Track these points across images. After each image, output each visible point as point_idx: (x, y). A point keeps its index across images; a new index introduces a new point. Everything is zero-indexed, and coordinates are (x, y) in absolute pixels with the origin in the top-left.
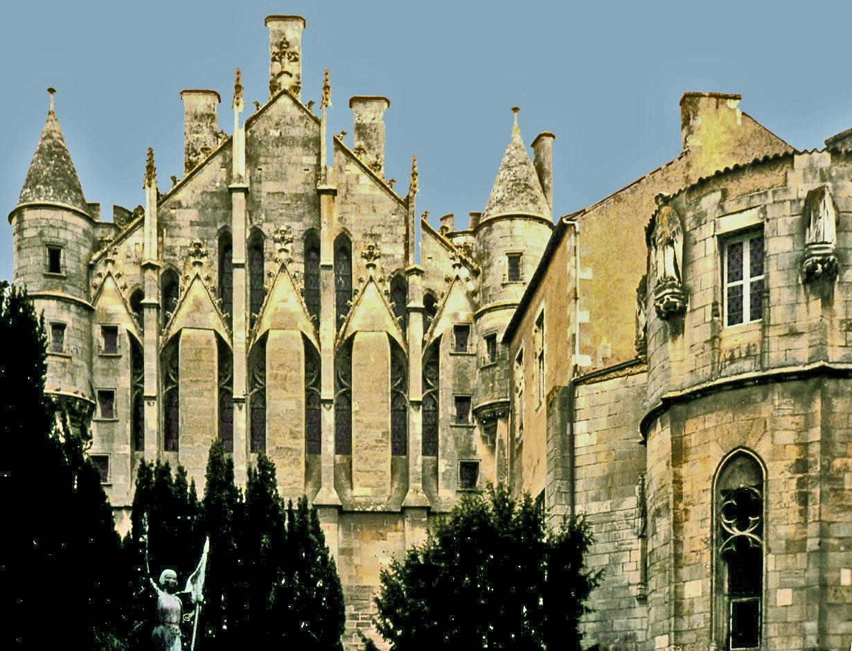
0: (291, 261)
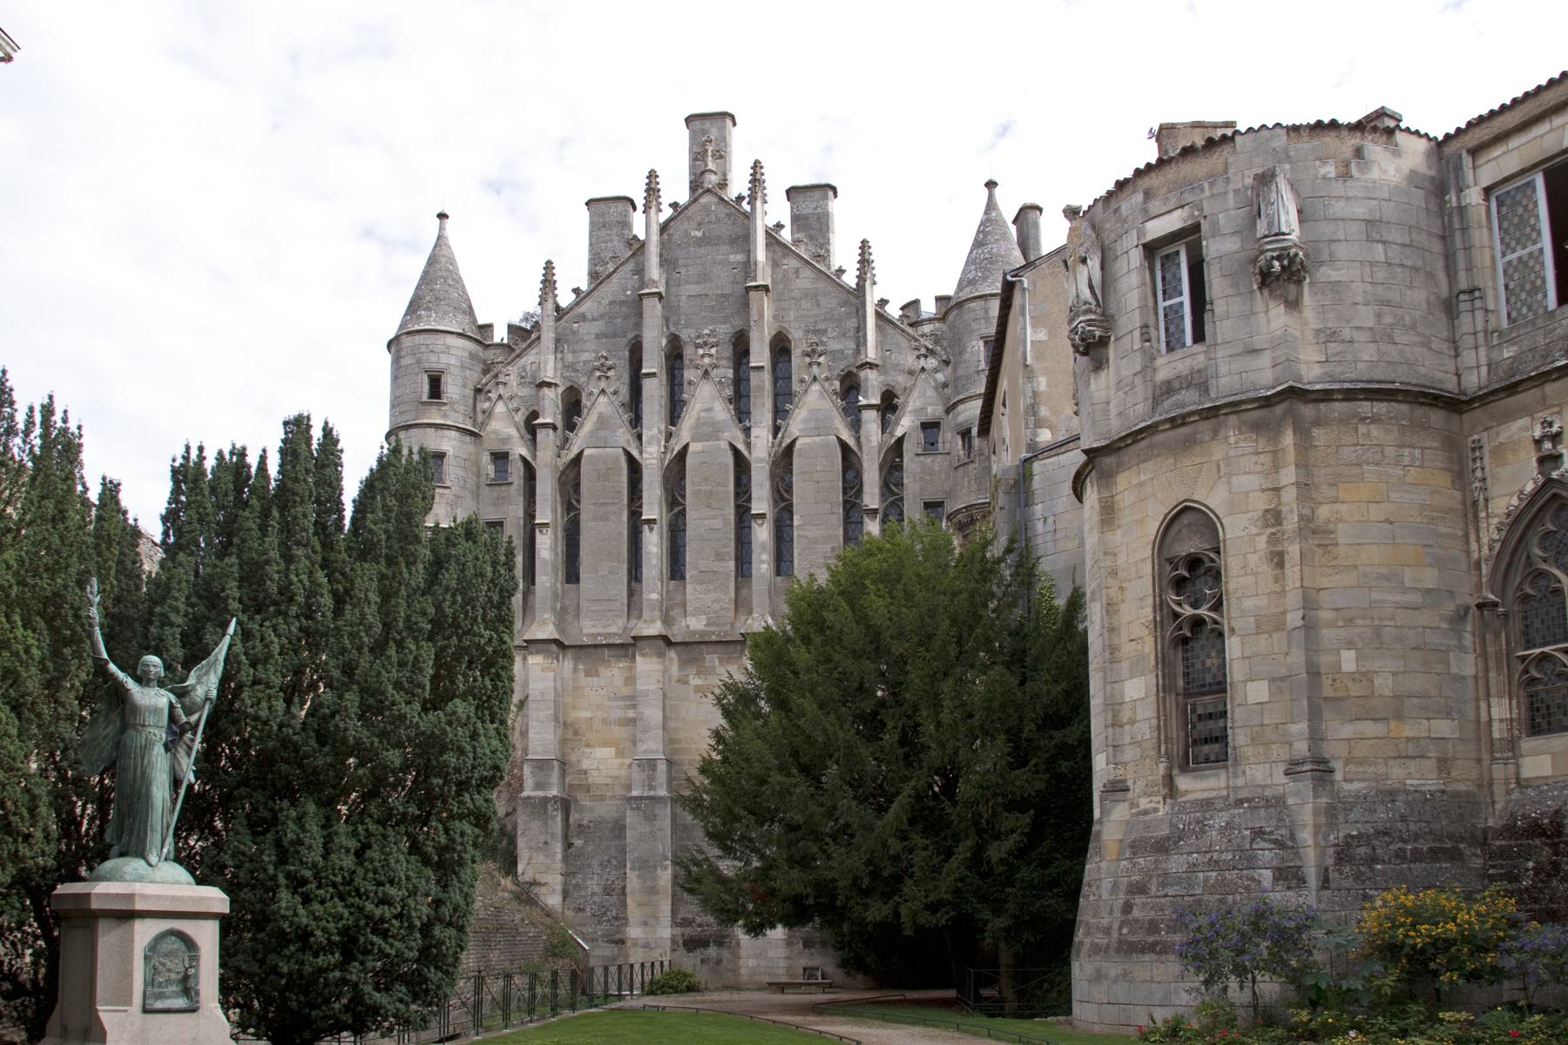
0: (716, 366)
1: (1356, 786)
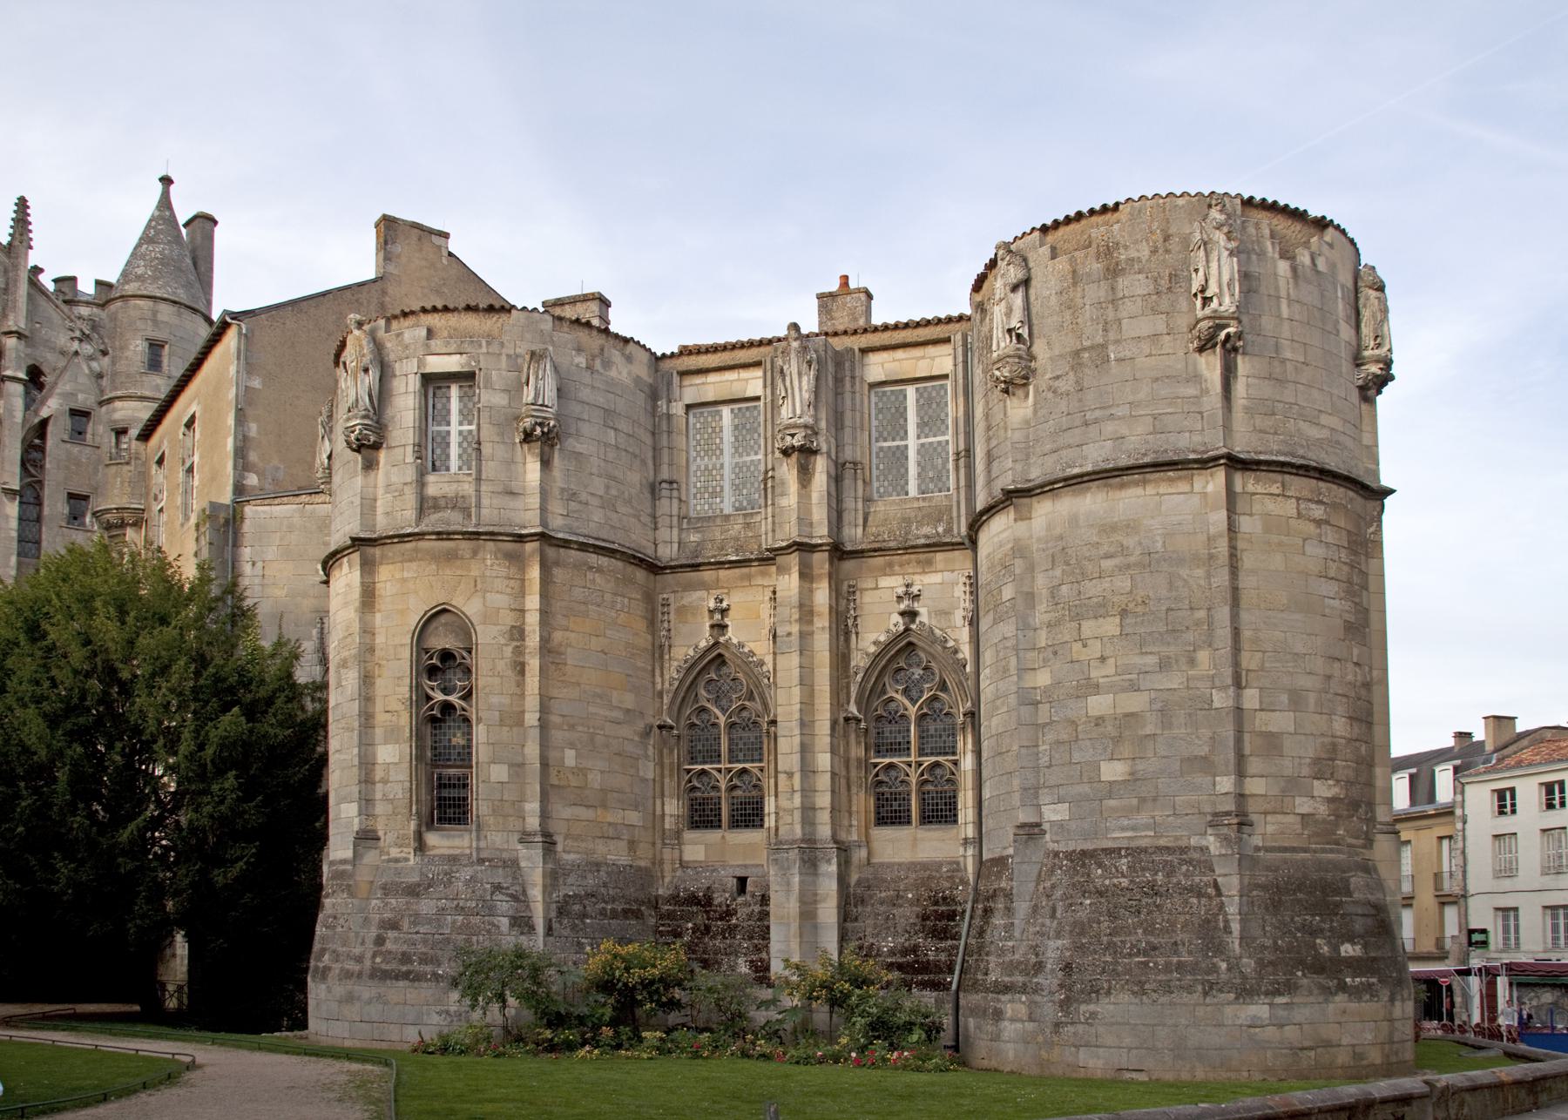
1: (572, 857)
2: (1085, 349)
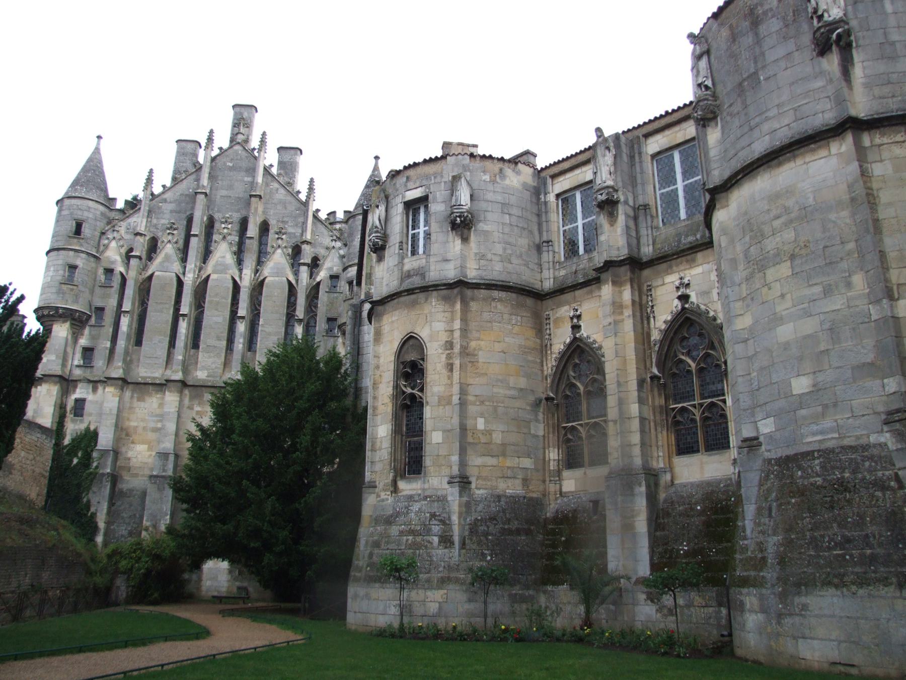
0: (230, 234)
2: (744, 80)
